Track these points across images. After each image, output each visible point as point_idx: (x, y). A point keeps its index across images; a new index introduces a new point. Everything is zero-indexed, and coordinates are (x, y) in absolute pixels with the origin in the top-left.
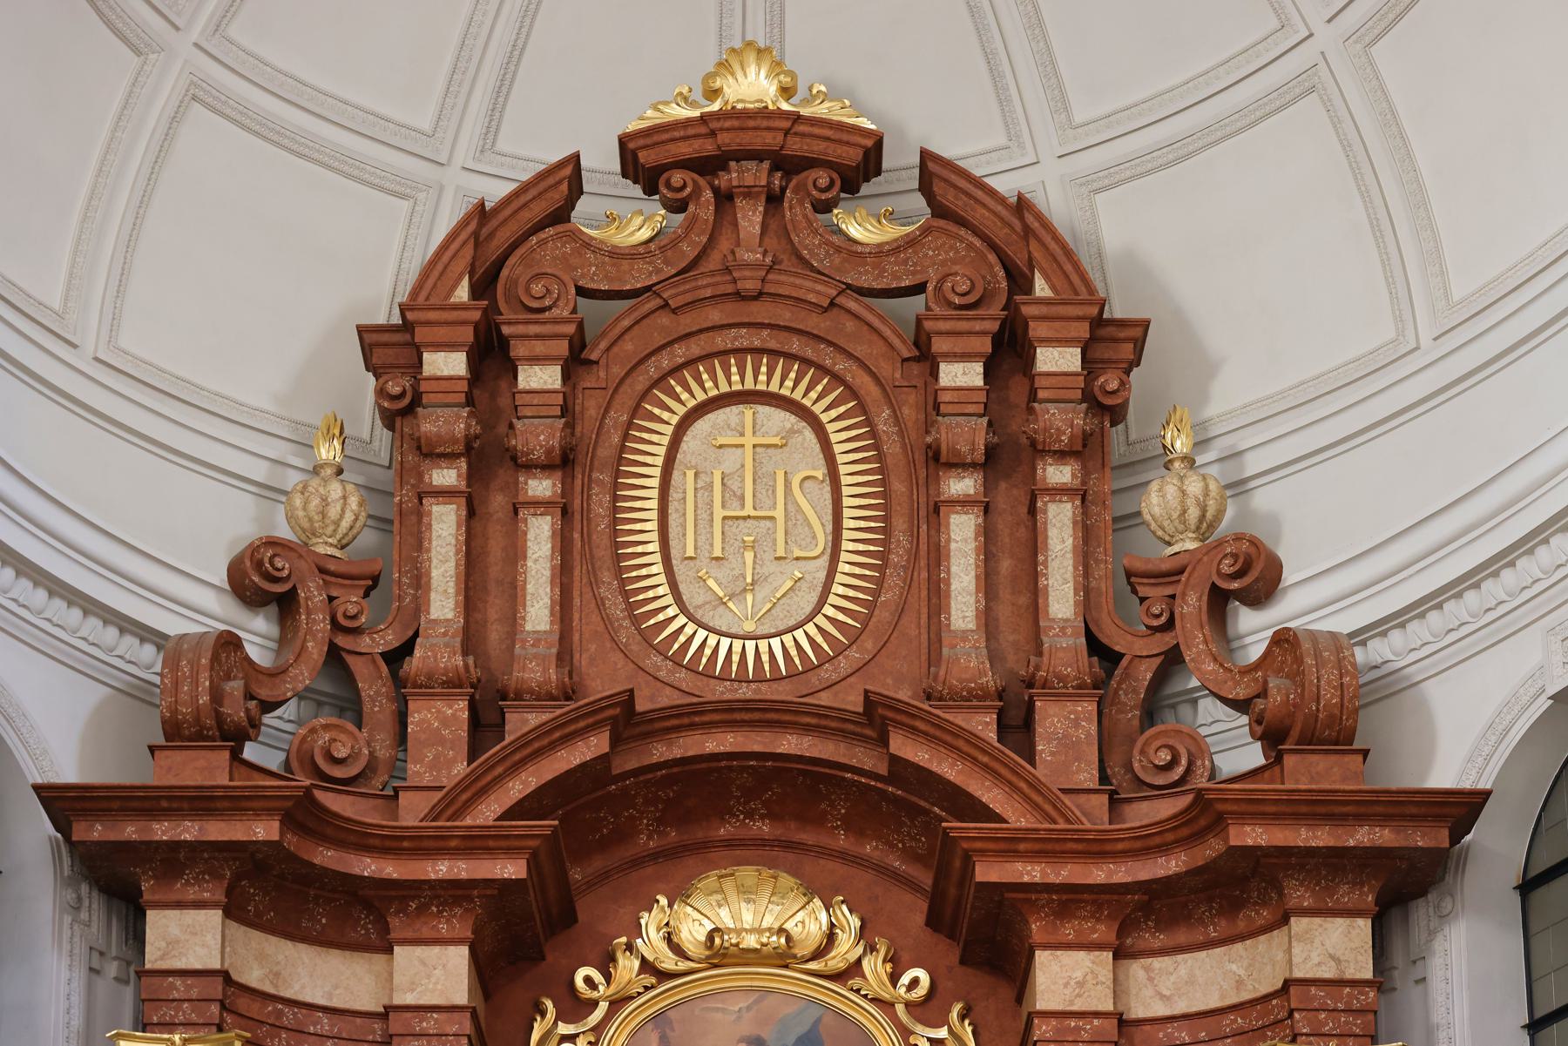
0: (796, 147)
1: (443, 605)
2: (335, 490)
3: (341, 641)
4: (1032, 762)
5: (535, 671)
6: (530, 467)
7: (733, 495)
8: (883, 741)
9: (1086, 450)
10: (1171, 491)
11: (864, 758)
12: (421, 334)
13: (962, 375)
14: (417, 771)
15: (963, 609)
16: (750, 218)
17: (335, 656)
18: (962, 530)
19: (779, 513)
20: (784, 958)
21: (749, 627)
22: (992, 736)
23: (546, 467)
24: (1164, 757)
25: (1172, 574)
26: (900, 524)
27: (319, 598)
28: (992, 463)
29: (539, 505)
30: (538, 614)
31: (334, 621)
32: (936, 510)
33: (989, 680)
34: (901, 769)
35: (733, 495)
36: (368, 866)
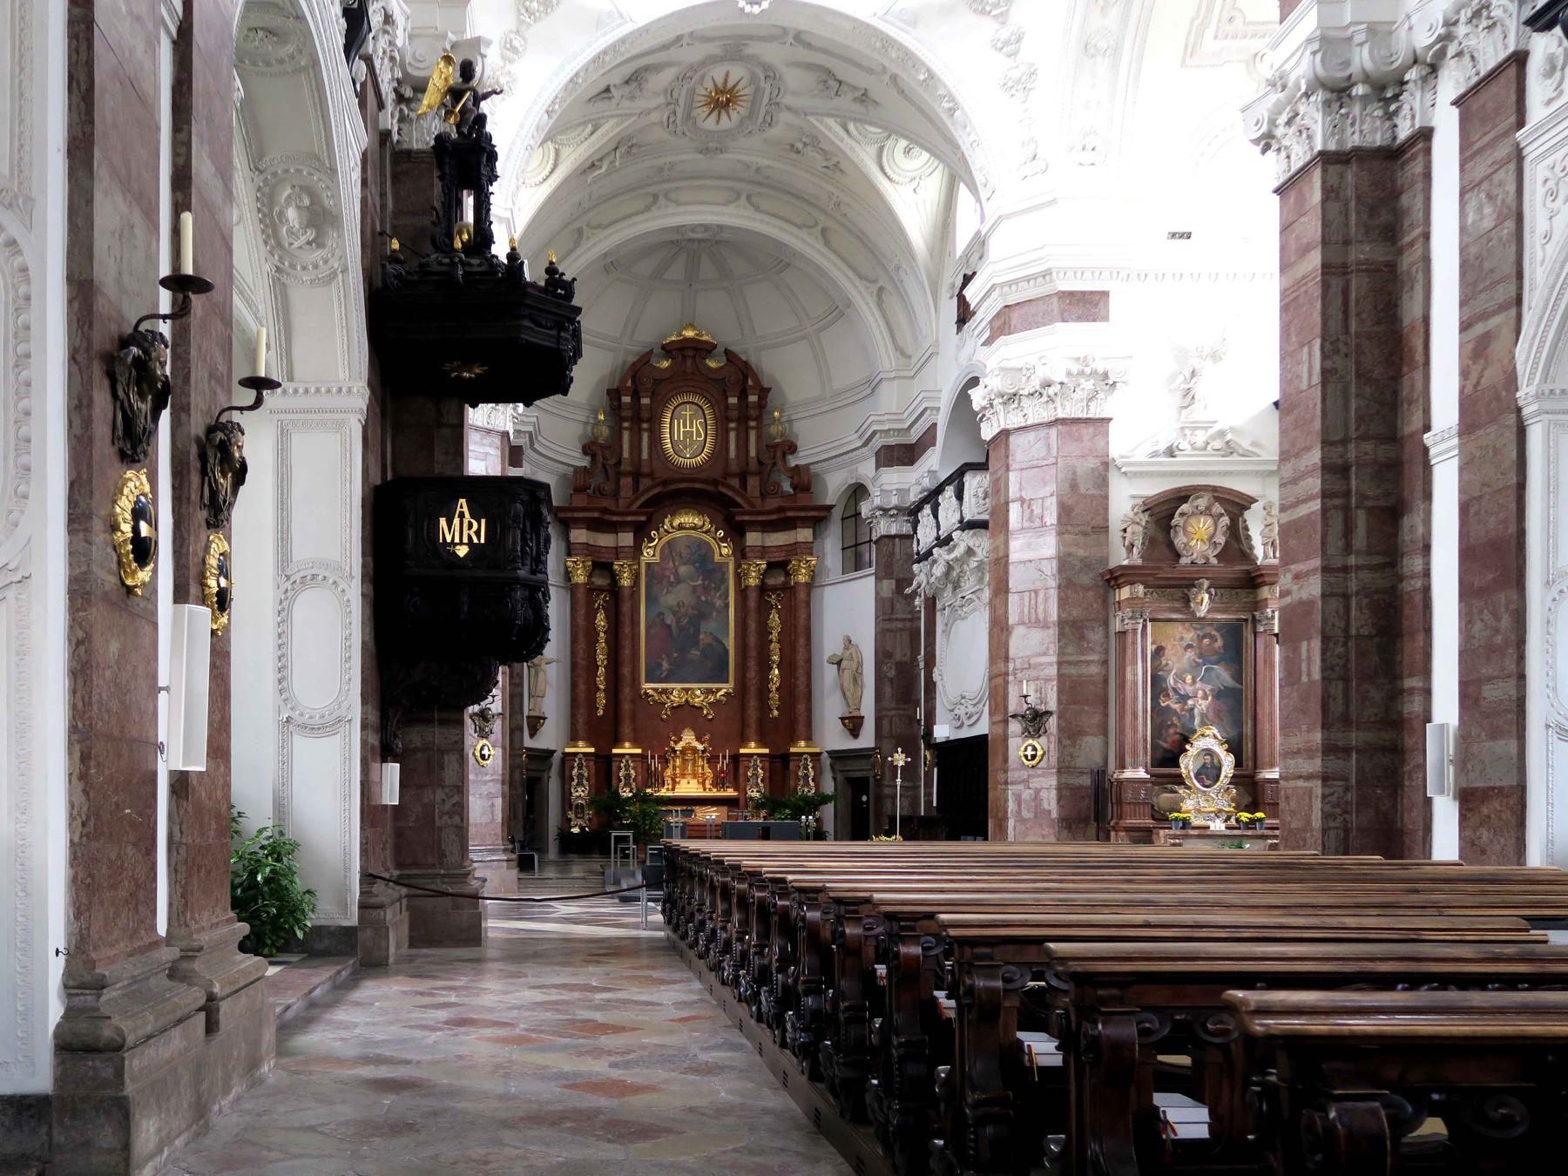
1: (626, 454)
5: (645, 470)
7: (685, 426)
9: (759, 418)
11: (710, 488)
13: (733, 400)
14: (622, 494)
15: (732, 454)
16: (689, 362)
18: (732, 435)
20: (695, 528)
22: (738, 486)
25: (777, 445)
27: (599, 452)
28: (738, 420)
29: (645, 430)
30: (645, 455)
32: (727, 431)
35: (685, 426)
36: (615, 518)
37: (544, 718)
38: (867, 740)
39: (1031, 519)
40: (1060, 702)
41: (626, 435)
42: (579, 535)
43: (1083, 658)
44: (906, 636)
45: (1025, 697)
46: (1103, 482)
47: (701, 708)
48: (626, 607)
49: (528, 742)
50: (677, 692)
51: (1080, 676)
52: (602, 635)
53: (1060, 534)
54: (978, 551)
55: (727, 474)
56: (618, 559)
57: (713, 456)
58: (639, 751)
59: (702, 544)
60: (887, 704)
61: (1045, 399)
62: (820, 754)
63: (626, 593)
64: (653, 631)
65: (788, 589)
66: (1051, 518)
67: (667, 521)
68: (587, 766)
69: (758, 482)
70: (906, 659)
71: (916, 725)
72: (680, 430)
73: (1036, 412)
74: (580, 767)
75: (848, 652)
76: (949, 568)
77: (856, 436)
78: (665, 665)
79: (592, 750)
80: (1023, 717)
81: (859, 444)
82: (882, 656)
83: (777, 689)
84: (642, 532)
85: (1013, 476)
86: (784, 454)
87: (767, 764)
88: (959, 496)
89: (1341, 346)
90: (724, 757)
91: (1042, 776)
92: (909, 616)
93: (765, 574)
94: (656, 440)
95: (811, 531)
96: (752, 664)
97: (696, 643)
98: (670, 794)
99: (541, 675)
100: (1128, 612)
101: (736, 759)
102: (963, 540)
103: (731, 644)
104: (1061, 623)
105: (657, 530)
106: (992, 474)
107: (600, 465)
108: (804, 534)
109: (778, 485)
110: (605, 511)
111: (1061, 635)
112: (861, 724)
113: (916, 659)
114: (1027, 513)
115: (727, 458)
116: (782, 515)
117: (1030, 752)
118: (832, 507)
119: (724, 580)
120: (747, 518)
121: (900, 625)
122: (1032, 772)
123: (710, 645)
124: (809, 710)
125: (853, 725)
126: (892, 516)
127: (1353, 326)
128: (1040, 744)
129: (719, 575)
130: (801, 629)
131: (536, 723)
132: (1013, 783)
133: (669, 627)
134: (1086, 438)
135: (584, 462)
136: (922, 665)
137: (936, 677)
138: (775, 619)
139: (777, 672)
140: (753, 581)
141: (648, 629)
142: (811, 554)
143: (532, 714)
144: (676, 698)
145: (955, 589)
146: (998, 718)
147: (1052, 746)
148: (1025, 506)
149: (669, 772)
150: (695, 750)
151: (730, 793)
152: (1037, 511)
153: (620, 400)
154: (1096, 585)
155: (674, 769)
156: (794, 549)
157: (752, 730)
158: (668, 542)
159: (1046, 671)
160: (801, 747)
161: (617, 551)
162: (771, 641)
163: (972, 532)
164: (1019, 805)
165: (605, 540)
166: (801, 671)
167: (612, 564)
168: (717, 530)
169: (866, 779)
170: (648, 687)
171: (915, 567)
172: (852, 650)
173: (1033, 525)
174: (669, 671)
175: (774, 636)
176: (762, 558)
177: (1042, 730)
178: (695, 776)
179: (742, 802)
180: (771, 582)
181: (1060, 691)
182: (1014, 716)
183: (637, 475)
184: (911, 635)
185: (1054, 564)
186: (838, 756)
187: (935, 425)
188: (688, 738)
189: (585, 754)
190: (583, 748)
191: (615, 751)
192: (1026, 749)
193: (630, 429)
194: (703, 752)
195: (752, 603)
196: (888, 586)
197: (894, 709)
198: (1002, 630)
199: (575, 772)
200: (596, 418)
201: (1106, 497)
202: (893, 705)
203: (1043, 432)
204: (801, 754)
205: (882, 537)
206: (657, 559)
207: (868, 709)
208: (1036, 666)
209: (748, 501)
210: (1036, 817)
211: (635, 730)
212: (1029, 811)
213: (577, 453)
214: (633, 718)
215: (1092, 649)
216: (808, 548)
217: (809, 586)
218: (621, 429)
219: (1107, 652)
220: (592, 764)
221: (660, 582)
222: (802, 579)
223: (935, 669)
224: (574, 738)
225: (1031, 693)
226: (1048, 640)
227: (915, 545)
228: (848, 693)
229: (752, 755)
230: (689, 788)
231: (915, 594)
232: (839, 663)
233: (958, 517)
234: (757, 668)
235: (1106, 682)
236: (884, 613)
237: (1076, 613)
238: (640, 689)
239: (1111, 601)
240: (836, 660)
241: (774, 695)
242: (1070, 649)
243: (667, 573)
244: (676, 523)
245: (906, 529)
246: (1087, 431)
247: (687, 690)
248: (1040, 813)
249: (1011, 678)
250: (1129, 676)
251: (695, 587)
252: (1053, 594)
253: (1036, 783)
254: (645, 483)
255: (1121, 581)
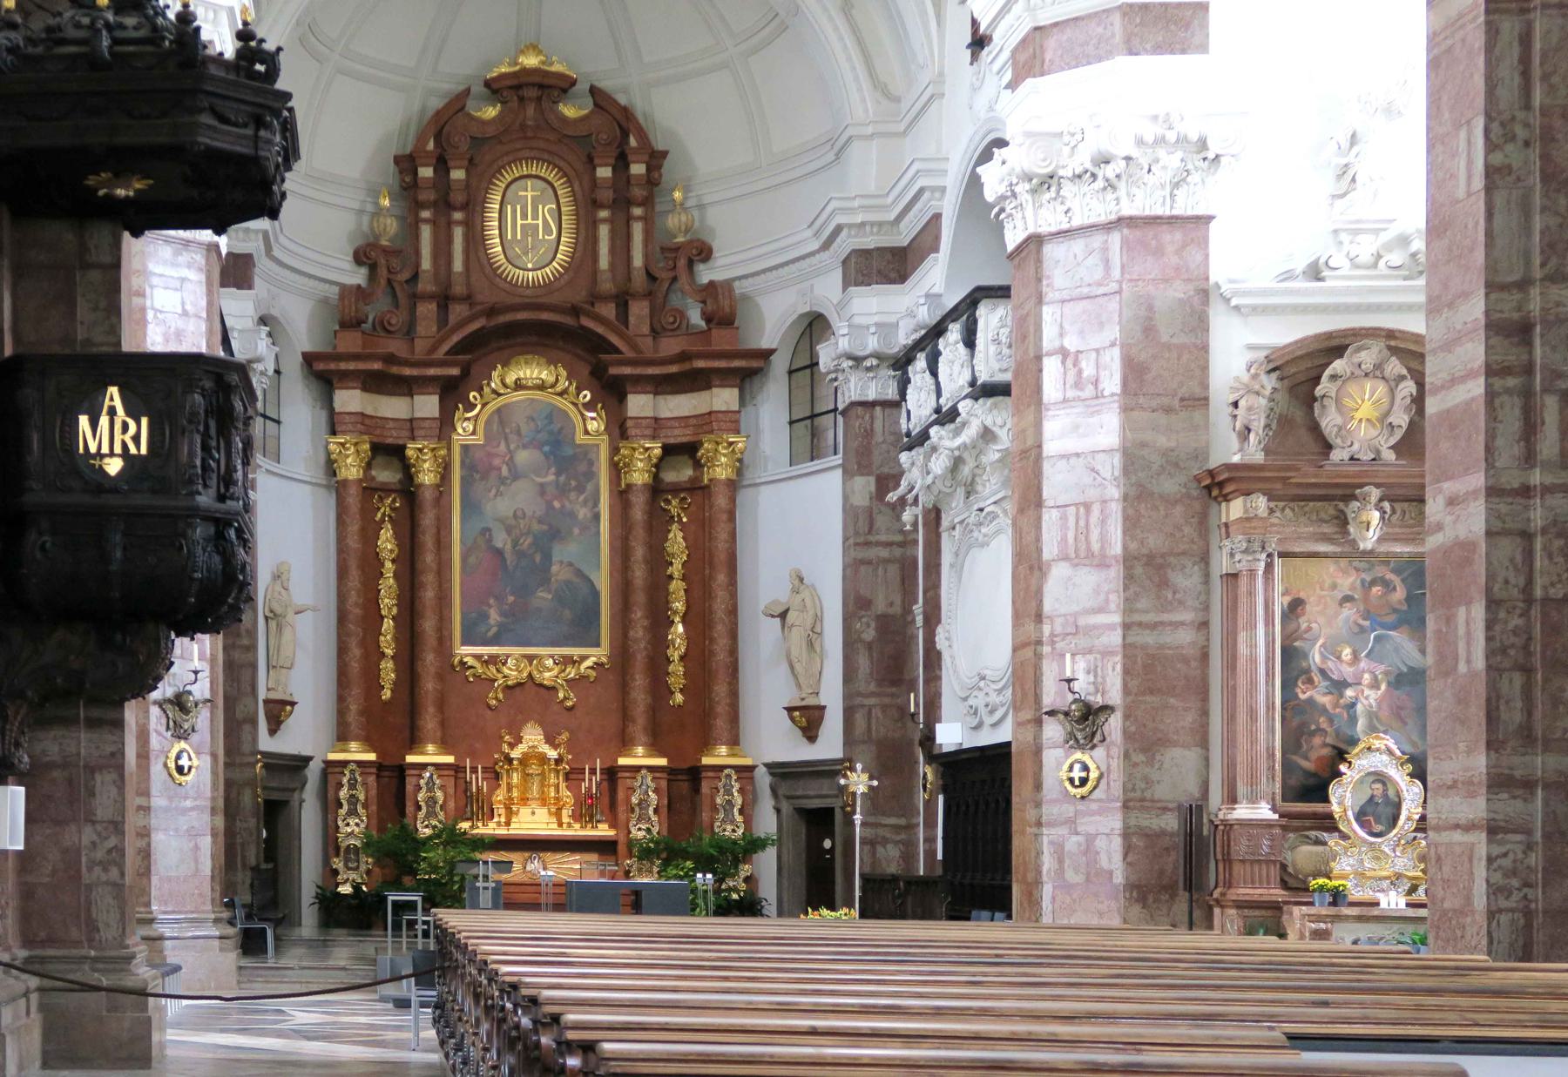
0: (546, 81)
1: (426, 264)
2: (389, 221)
3: (391, 277)
4: (627, 328)
5: (458, 289)
6: (456, 209)
7: (524, 216)
8: (578, 317)
10: (676, 220)
11: (568, 320)
12: (418, 161)
14: (421, 329)
15: (604, 263)
17: (389, 281)
18: (604, 231)
19: (540, 222)
20: (542, 387)
21: (530, 266)
23: (464, 207)
24: (671, 320)
25: (677, 249)
26: (582, 226)
27: (383, 261)
29: (458, 223)
30: (458, 265)
31: (389, 271)
32: (594, 224)
33: (614, 291)
34: (583, 328)
35: (524, 216)
37: (293, 704)
38: (829, 745)
39: (1078, 385)
40: (1126, 690)
41: (426, 232)
42: (349, 400)
43: (1166, 617)
44: (893, 570)
45: (1069, 681)
46: (1199, 323)
47: (553, 689)
48: (428, 519)
49: (266, 743)
50: (513, 662)
51: (1162, 647)
52: (388, 565)
53: (1126, 409)
54: (1003, 434)
55: (595, 297)
56: (413, 439)
57: (573, 267)
58: (450, 759)
59: (554, 414)
60: (865, 683)
61: (1100, 183)
62: (751, 769)
63: (428, 496)
64: (472, 560)
65: (698, 489)
66: (1112, 383)
67: (495, 374)
68: (364, 784)
69: (646, 311)
70: (897, 609)
71: (910, 724)
72: (517, 223)
73: (1088, 206)
74: (352, 786)
75: (798, 598)
76: (957, 462)
77: (809, 233)
78: (494, 616)
79: (372, 757)
80: (1066, 714)
81: (815, 245)
82: (856, 604)
83: (682, 658)
84: (453, 393)
85: (1048, 312)
86: (691, 264)
87: (664, 784)
88: (970, 342)
89: (1521, 132)
90: (593, 771)
91: (1099, 813)
92: (899, 538)
93: (657, 466)
94: (476, 240)
95: (736, 391)
96: (638, 614)
97: (545, 581)
98: (502, 831)
99: (287, 633)
100: (1239, 541)
101: (612, 774)
102: (976, 414)
103: (603, 581)
104: (1128, 560)
105: (480, 390)
106: (1015, 309)
107: (383, 282)
108: (724, 398)
109: (681, 314)
110: (390, 359)
111: (1129, 578)
112: (821, 719)
113: (910, 612)
114: (1072, 373)
115: (595, 271)
116: (686, 366)
117: (1077, 774)
118: (771, 352)
119: (591, 475)
120: (627, 370)
121: (884, 553)
122: (1081, 806)
123: (568, 583)
124: (734, 694)
125: (808, 720)
126: (868, 369)
127: (1537, 98)
128: (1095, 759)
129: (582, 467)
130: (721, 556)
131: (278, 712)
132: (1051, 824)
133: (499, 553)
134: (1170, 249)
135: (358, 277)
136: (919, 620)
137: (941, 642)
138: (676, 541)
139: (680, 628)
140: (639, 476)
141: (464, 559)
142: (737, 432)
143: (273, 696)
144: (512, 672)
145: (968, 494)
146: (1027, 715)
147: (1114, 763)
148: (1069, 363)
149: (500, 795)
150: (543, 759)
151: (603, 831)
152: (1088, 370)
153: (416, 173)
154: (1188, 496)
155: (510, 789)
156: (707, 421)
157: (638, 727)
158: (499, 411)
159: (1104, 640)
160: (720, 755)
161: (412, 426)
162: (671, 577)
163: (990, 401)
164: (1061, 861)
165: (392, 407)
166: (720, 627)
167: (403, 447)
168: (579, 390)
169: (829, 812)
170: (465, 652)
171: (904, 457)
172: (806, 594)
173: (1083, 395)
174: (500, 625)
175: (676, 569)
176: (654, 438)
177: (1098, 737)
178: (544, 802)
179: (622, 848)
180: (670, 477)
181: (1126, 672)
182: (1051, 713)
183: (444, 300)
184: (903, 569)
185: (1117, 460)
186: (783, 773)
187: (937, 217)
188: (533, 738)
189: (360, 763)
190: (358, 753)
191: (410, 759)
192: (1071, 769)
193: (433, 222)
194: (558, 761)
195: (638, 513)
196: (864, 486)
197: (873, 694)
198: (1031, 568)
199: (344, 793)
200: (377, 204)
201: (1205, 348)
202: (872, 687)
203: (1097, 240)
204: (721, 768)
205: (853, 404)
206: (479, 439)
207: (832, 695)
208: (1090, 630)
209: (634, 347)
210: (1088, 880)
211: (443, 724)
212: (1077, 872)
213: (346, 262)
214: (441, 704)
215: (1181, 602)
216: (732, 422)
217: (733, 485)
218: (417, 221)
219: (1206, 608)
220: (372, 779)
221: (484, 477)
222: (721, 470)
223: (939, 630)
224: (342, 736)
225: (1081, 675)
226: (1106, 587)
227: (903, 421)
228: (798, 667)
229: (638, 769)
230: (534, 821)
231: (902, 501)
232: (783, 616)
233: (967, 376)
234: (646, 623)
235: (1205, 656)
236: (857, 533)
237: (1155, 542)
238: (452, 656)
239: (1213, 521)
240: (780, 610)
241: (677, 668)
242: (1143, 604)
243: (497, 462)
244: (511, 379)
245: (891, 393)
246: (1172, 238)
247: (530, 658)
248: (1095, 874)
249: (1046, 649)
250: (1243, 649)
251: (542, 485)
252: (1116, 509)
253: (1087, 825)
254: (458, 311)
255: (1229, 489)
